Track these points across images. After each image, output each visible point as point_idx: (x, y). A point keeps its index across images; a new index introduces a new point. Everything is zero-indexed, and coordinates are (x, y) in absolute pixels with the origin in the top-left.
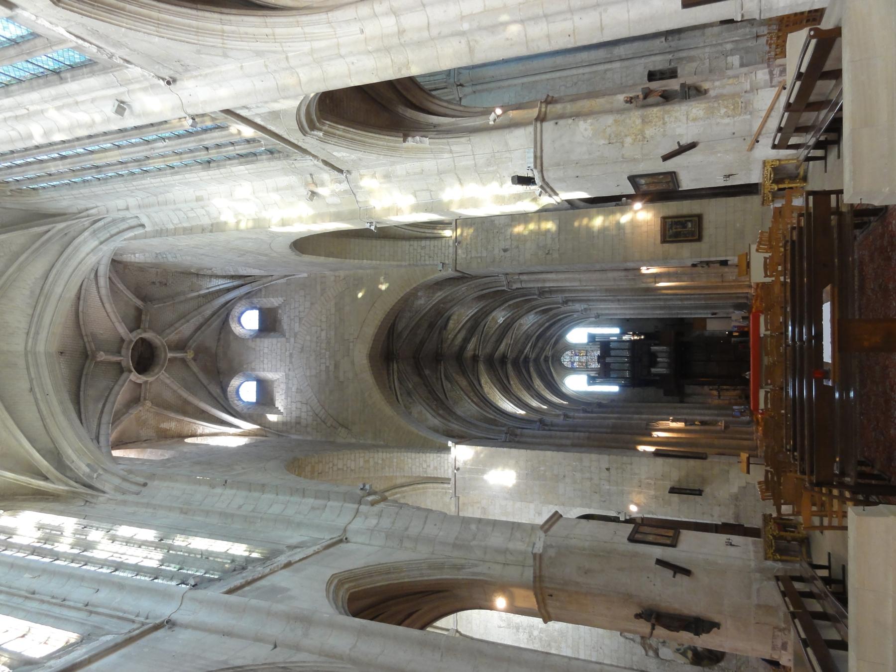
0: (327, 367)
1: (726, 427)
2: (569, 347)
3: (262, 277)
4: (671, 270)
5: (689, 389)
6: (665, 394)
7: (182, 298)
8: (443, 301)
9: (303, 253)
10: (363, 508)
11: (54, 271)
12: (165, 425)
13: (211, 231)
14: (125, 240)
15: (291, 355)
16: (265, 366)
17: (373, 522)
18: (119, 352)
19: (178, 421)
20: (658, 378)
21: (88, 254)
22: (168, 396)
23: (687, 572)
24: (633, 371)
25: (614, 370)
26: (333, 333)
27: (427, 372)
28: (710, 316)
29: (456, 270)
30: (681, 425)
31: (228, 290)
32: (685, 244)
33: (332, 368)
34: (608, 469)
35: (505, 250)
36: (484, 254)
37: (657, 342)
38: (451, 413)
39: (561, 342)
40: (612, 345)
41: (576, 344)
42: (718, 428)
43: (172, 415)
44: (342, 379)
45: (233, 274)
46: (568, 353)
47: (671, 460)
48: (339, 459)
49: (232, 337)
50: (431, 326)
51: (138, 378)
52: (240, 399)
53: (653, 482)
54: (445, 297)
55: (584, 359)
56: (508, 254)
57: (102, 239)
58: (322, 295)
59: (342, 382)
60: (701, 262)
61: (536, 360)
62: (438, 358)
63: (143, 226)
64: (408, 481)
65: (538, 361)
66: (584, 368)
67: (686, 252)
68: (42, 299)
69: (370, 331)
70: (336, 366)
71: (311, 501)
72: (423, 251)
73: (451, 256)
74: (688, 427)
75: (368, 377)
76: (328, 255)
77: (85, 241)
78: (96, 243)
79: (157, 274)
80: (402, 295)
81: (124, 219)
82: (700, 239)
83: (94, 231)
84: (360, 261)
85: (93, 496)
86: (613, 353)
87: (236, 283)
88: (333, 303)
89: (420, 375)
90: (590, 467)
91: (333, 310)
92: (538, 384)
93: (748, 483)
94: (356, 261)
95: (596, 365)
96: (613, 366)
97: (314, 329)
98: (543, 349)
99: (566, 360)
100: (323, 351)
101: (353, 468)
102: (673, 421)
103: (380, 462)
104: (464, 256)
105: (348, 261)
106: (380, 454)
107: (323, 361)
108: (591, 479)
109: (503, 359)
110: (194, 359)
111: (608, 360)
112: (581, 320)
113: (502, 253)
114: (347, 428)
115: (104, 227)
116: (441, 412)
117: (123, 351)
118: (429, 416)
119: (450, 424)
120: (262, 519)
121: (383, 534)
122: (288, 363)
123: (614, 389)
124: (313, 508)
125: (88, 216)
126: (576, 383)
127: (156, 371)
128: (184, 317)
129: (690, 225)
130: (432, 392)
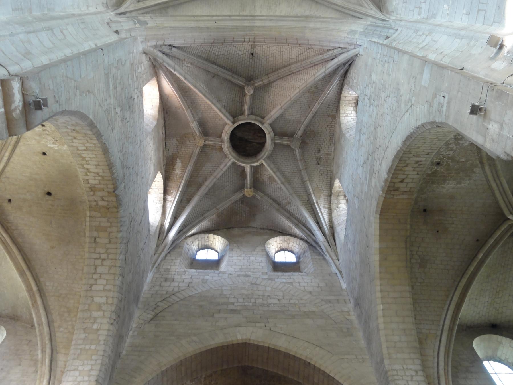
0: (233, 304)
3: (336, 252)
7: (306, 178)
9: (381, 214)
12: (179, 164)
18: (251, 113)
19: (182, 177)
22: (208, 168)
26: (276, 308)
31: (318, 222)
33: (231, 307)
43: (189, 168)
44: (216, 316)
48: (110, 267)
49: (266, 237)
52: (199, 249)
58: (322, 300)
59: (213, 316)
64: (59, 370)
69: (281, 343)
70: (233, 311)
75: (219, 339)
76: (381, 251)
79: (328, 154)
80: (337, 378)
84: (379, 301)
88: (314, 309)
94: (379, 295)
97: (281, 294)
100: (253, 300)
101: (94, 288)
103: (95, 326)
105: (378, 282)
106: (106, 327)
107: (241, 300)
110: (244, 200)
114: (152, 319)
122: (239, 273)
127: (233, 154)
128: (287, 180)
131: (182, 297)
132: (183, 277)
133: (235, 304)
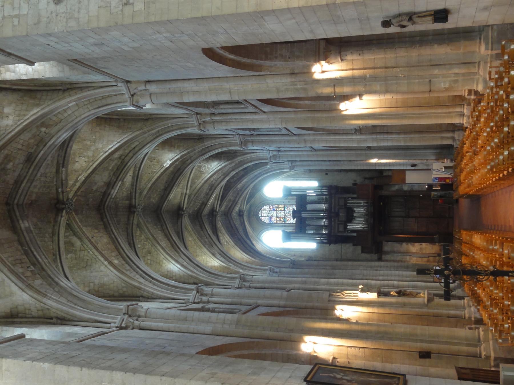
1: (430, 300)
2: (265, 202)
4: (357, 73)
5: (387, 247)
8: (42, 122)
20: (355, 234)
24: (329, 226)
25: (310, 225)
27: (24, 225)
28: (409, 167)
30: (373, 296)
36: (24, 11)
37: (355, 196)
38: (53, 283)
39: (257, 196)
40: (308, 199)
41: (274, 199)
42: (419, 300)
46: (266, 207)
50: (30, 159)
55: (281, 214)
60: (400, 15)
61: (227, 214)
62: (57, 206)
65: (225, 215)
74: (383, 299)
86: (309, 207)
89: (14, 229)
92: (226, 238)
95: (293, 221)
98: (234, 203)
99: (264, 214)
102: (363, 291)
109: (178, 212)
111: (304, 214)
112: (278, 174)
116: (38, 282)
118: (15, 288)
119: (44, 300)
123: (309, 245)
126: (272, 240)
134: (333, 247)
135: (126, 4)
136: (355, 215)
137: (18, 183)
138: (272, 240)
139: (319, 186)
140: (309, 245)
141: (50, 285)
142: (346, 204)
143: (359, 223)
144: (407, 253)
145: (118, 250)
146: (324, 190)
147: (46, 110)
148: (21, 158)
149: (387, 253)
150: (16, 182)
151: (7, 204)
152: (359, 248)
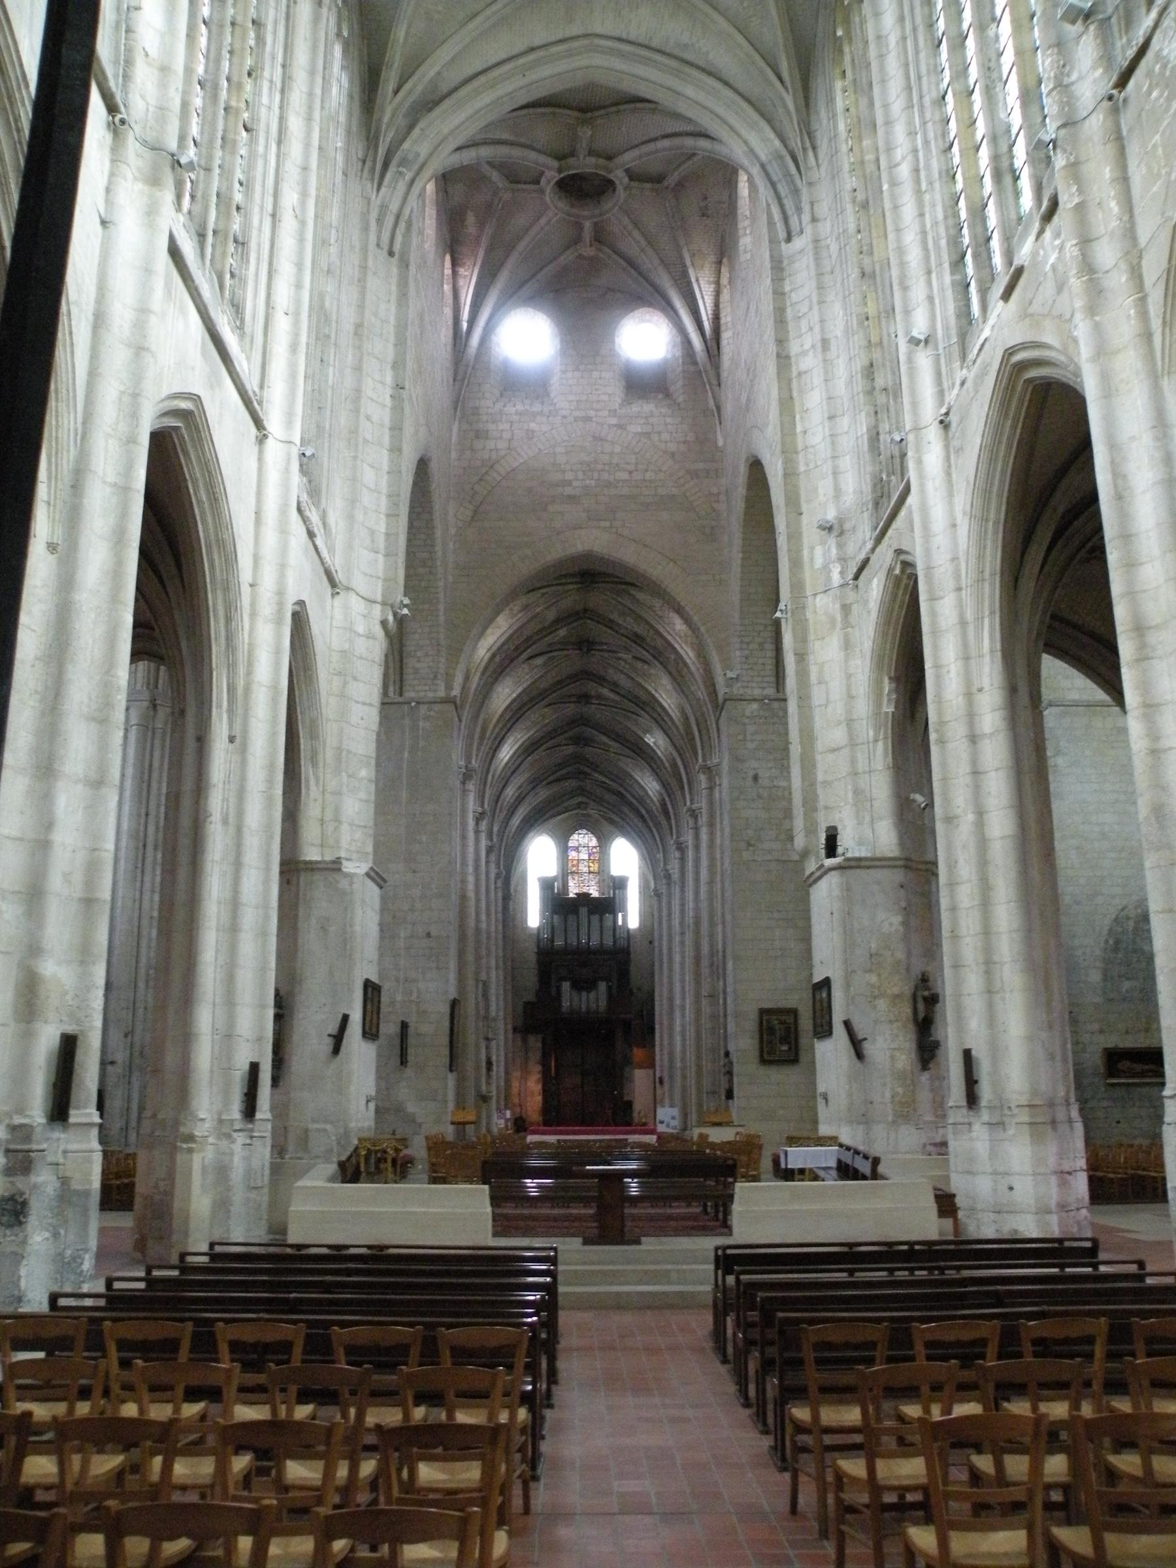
0: (569, 483)
2: (604, 842)
5: (535, 1042)
6: (527, 1004)
10: (377, 611)
11: (719, 86)
13: (778, 356)
14: (768, 205)
15: (588, 419)
16: (569, 375)
17: (361, 629)
18: (591, 152)
21: (745, 142)
23: (336, 1050)
24: (566, 951)
26: (626, 491)
29: (725, 700)
32: (756, 1042)
33: (568, 491)
34: (429, 935)
35: (756, 778)
39: (612, 828)
44: (550, 508)
45: (723, 321)
46: (594, 842)
47: (447, 1024)
50: (638, 639)
51: (549, 182)
53: (414, 997)
54: (685, 664)
55: (583, 868)
56: (749, 782)
57: (769, 168)
58: (688, 472)
59: (545, 510)
61: (582, 791)
63: (789, 239)
66: (566, 872)
67: (743, 1043)
68: (674, 64)
70: (572, 499)
71: (382, 527)
72: (754, 646)
73: (749, 691)
75: (556, 552)
77: (765, 140)
78: (763, 158)
81: (799, 210)
82: (764, 1061)
83: (781, 157)
85: (373, 170)
86: (595, 919)
87: (707, 326)
88: (675, 491)
90: (430, 909)
91: (661, 491)
92: (543, 794)
93: (420, 1125)
96: (571, 918)
99: (583, 839)
100: (596, 475)
104: (748, 713)
107: (580, 475)
108: (412, 910)
111: (583, 911)
113: (751, 773)
115: (787, 174)
116: (498, 659)
117: (592, 160)
120: (355, 458)
121: (347, 646)
122: (577, 414)
124: (372, 533)
125: (804, 149)
126: (540, 856)
127: (561, 204)
129: (785, 1048)
130: (529, 642)
131: (503, 472)
132: (501, 427)
133: (575, 484)
134: (532, 958)
135: (749, 844)
136: (584, 994)
137: (611, 624)
138: (540, 856)
139: (628, 931)
140: (534, 916)
141: (494, 671)
142: (602, 979)
143: (570, 999)
144: (526, 1072)
145: (531, 700)
146: (622, 943)
147: (693, 669)
148: (640, 629)
149: (525, 1040)
150: (612, 621)
151: (586, 610)
152: (531, 997)
